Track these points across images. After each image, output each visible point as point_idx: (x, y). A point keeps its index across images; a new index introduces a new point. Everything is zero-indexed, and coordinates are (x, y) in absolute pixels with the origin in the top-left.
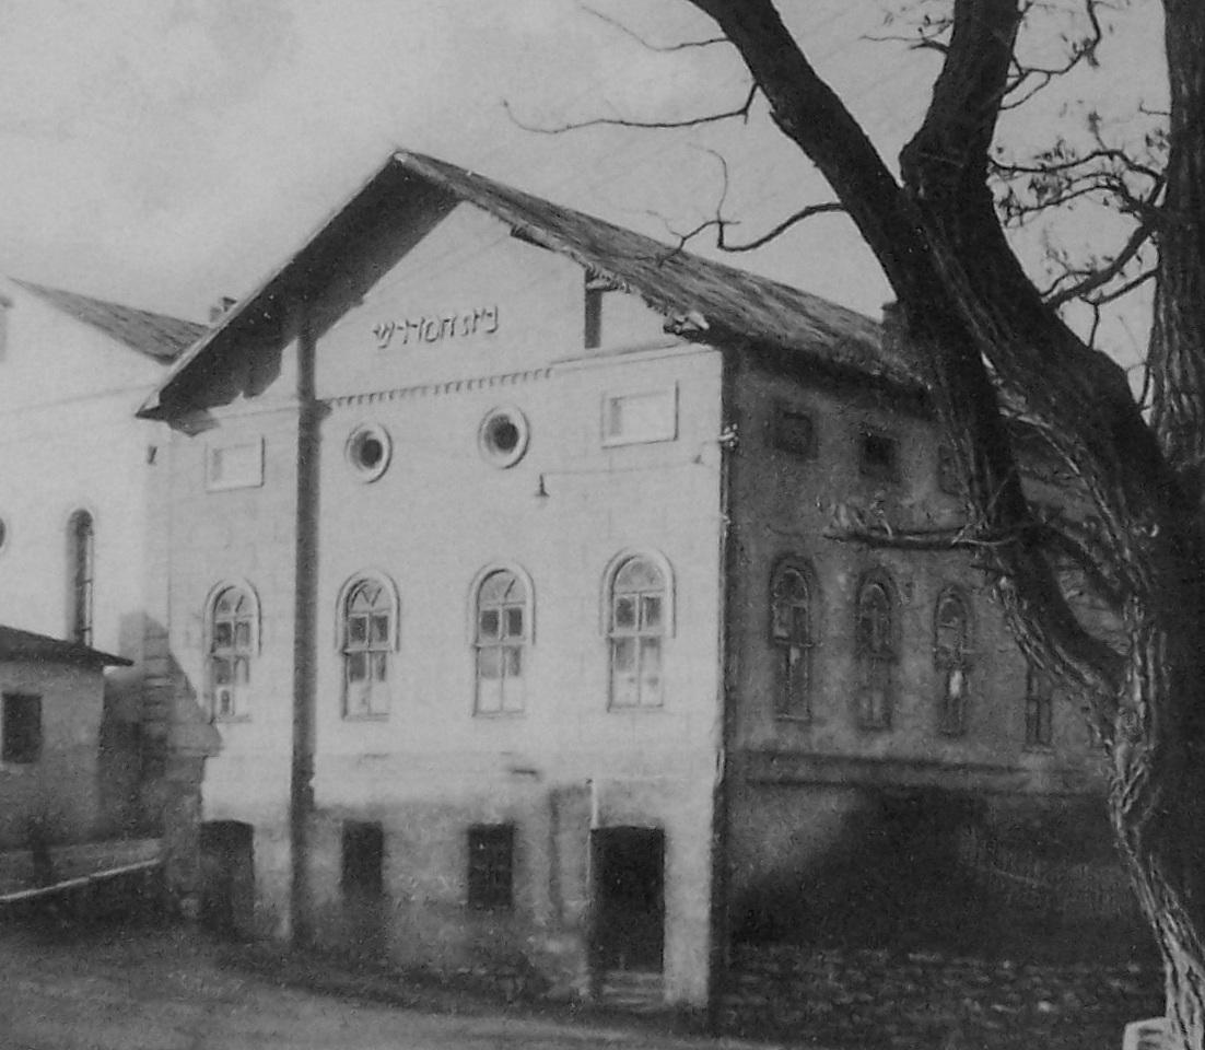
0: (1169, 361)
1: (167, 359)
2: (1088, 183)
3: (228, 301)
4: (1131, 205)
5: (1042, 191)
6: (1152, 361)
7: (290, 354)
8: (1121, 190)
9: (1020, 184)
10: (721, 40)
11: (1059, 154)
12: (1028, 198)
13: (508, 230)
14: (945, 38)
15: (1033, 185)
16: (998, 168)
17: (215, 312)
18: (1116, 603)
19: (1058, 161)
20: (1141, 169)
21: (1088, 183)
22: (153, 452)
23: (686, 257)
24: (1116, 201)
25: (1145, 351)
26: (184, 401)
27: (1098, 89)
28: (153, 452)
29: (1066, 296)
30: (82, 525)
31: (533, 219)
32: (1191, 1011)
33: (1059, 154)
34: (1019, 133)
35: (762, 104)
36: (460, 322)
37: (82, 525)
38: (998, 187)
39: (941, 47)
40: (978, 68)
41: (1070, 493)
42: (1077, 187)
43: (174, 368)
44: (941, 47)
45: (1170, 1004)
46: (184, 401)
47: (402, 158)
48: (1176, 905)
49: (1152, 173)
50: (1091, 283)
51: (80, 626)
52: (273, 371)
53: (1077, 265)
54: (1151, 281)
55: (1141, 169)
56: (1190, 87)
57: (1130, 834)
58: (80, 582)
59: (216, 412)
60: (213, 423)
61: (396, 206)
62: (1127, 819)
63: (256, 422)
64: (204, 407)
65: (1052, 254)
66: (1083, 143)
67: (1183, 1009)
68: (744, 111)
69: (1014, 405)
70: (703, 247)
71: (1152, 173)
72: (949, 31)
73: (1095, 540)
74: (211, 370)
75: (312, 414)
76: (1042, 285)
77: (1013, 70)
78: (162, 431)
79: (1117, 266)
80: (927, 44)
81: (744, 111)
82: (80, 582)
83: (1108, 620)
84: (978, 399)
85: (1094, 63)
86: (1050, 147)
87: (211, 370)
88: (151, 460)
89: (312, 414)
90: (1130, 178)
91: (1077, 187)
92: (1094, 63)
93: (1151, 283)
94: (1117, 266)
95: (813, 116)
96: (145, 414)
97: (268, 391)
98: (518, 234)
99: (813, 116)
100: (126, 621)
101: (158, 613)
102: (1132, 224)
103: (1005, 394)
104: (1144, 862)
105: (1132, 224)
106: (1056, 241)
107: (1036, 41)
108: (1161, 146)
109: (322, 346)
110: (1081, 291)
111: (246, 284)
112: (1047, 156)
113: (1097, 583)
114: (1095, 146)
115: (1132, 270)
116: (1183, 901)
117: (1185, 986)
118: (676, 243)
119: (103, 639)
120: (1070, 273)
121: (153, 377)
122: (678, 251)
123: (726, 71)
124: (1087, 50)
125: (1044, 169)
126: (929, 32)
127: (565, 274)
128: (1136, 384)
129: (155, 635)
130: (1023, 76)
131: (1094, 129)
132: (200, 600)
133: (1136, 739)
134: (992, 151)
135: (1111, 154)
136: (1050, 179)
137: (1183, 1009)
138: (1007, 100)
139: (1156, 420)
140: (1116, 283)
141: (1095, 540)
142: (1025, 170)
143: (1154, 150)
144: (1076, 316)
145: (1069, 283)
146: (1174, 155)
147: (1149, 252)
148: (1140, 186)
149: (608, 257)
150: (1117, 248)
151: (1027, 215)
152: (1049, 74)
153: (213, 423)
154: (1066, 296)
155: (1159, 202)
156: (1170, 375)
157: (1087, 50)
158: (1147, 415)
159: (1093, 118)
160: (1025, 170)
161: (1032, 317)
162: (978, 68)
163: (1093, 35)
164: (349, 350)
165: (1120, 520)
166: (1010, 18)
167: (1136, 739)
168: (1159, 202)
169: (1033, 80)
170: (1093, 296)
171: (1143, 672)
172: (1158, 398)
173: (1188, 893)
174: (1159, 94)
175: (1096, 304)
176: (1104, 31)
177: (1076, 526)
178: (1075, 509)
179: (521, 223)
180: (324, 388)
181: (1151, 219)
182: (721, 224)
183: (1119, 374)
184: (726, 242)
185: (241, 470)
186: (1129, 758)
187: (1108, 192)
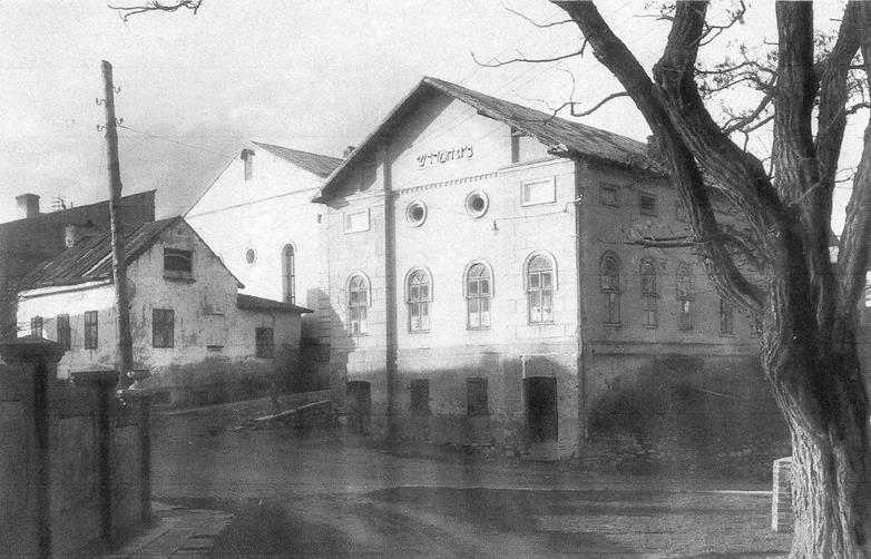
0: (782, 156)
1: (326, 175)
2: (742, 77)
3: (351, 148)
4: (761, 86)
5: (719, 81)
6: (774, 156)
7: (380, 170)
8: (757, 80)
9: (710, 78)
10: (622, 94)
11: (727, 65)
12: (713, 85)
13: (475, 111)
14: (673, 14)
15: (715, 79)
16: (699, 72)
17: (346, 153)
18: (761, 268)
19: (727, 68)
20: (766, 70)
21: (742, 77)
22: (320, 216)
23: (557, 119)
24: (754, 85)
25: (770, 152)
26: (333, 194)
27: (744, 35)
28: (320, 216)
29: (732, 129)
30: (289, 251)
31: (488, 106)
32: (804, 453)
33: (727, 65)
34: (709, 55)
35: (589, 49)
36: (456, 157)
37: (289, 251)
38: (699, 81)
39: (669, 18)
40: (690, 26)
41: (734, 218)
42: (736, 79)
43: (328, 180)
44: (669, 18)
45: (795, 449)
46: (333, 194)
47: (427, 81)
48: (795, 405)
49: (771, 71)
50: (743, 123)
51: (289, 295)
52: (371, 178)
53: (737, 115)
54: (773, 120)
55: (766, 70)
56: (788, 32)
57: (772, 374)
58: (289, 276)
59: (348, 199)
60: (347, 204)
61: (425, 101)
62: (771, 365)
63: (364, 204)
64: (342, 196)
65: (725, 111)
66: (738, 59)
67: (801, 451)
68: (581, 53)
69: (709, 180)
70: (565, 115)
71: (771, 71)
72: (674, 11)
73: (750, 239)
74: (345, 178)
75: (391, 197)
76: (721, 125)
77: (705, 28)
78: (322, 208)
79: (756, 115)
80: (664, 17)
81: (581, 53)
82: (289, 276)
83: (757, 276)
84: (695, 179)
85: (742, 22)
86: (722, 62)
87: (345, 178)
88: (319, 221)
89: (391, 197)
90: (760, 74)
91: (736, 79)
92: (742, 22)
93: (772, 122)
94: (756, 115)
95: (613, 53)
96: (314, 201)
97: (370, 188)
98: (480, 113)
99: (613, 53)
100: (310, 292)
101: (324, 287)
102: (762, 95)
103: (705, 175)
104: (779, 386)
105: (762, 95)
106: (728, 103)
107: (714, 14)
108: (775, 59)
109: (395, 168)
110: (739, 127)
111: (358, 142)
112: (721, 66)
113: (751, 258)
114: (743, 60)
115: (763, 116)
116: (798, 403)
117: (801, 442)
118: (552, 113)
119: (301, 300)
120: (734, 118)
121: (317, 184)
122: (553, 117)
123: (573, 34)
124: (739, 17)
125: (720, 72)
126: (665, 12)
127: (503, 130)
128: (767, 170)
129: (324, 299)
130: (709, 30)
131: (743, 53)
132: (343, 284)
133: (772, 330)
134: (696, 65)
135: (751, 64)
136: (723, 76)
137: (801, 451)
138: (702, 42)
139: (776, 184)
140: (756, 122)
141: (750, 239)
142: (711, 73)
143: (772, 61)
144: (737, 138)
145: (733, 123)
146: (781, 65)
147: (771, 107)
148: (766, 77)
149: (520, 122)
150: (755, 107)
151: (713, 94)
152: (722, 28)
153: (347, 204)
154: (732, 129)
155: (775, 84)
156: (783, 164)
157: (739, 17)
158: (772, 181)
159: (742, 48)
160: (711, 73)
161: (717, 138)
162: (690, 26)
163: (742, 9)
164: (407, 169)
165: (761, 231)
166: (702, 6)
167: (772, 330)
168: (775, 84)
169: (714, 32)
170: (745, 128)
171: (775, 298)
172: (777, 174)
173: (800, 399)
174: (773, 34)
175: (746, 132)
176: (747, 7)
177: (742, 235)
178: (740, 226)
179: (481, 108)
180: (396, 185)
181: (771, 92)
182: (572, 104)
183: (759, 163)
184: (575, 112)
185: (360, 223)
186: (770, 337)
187: (750, 81)
